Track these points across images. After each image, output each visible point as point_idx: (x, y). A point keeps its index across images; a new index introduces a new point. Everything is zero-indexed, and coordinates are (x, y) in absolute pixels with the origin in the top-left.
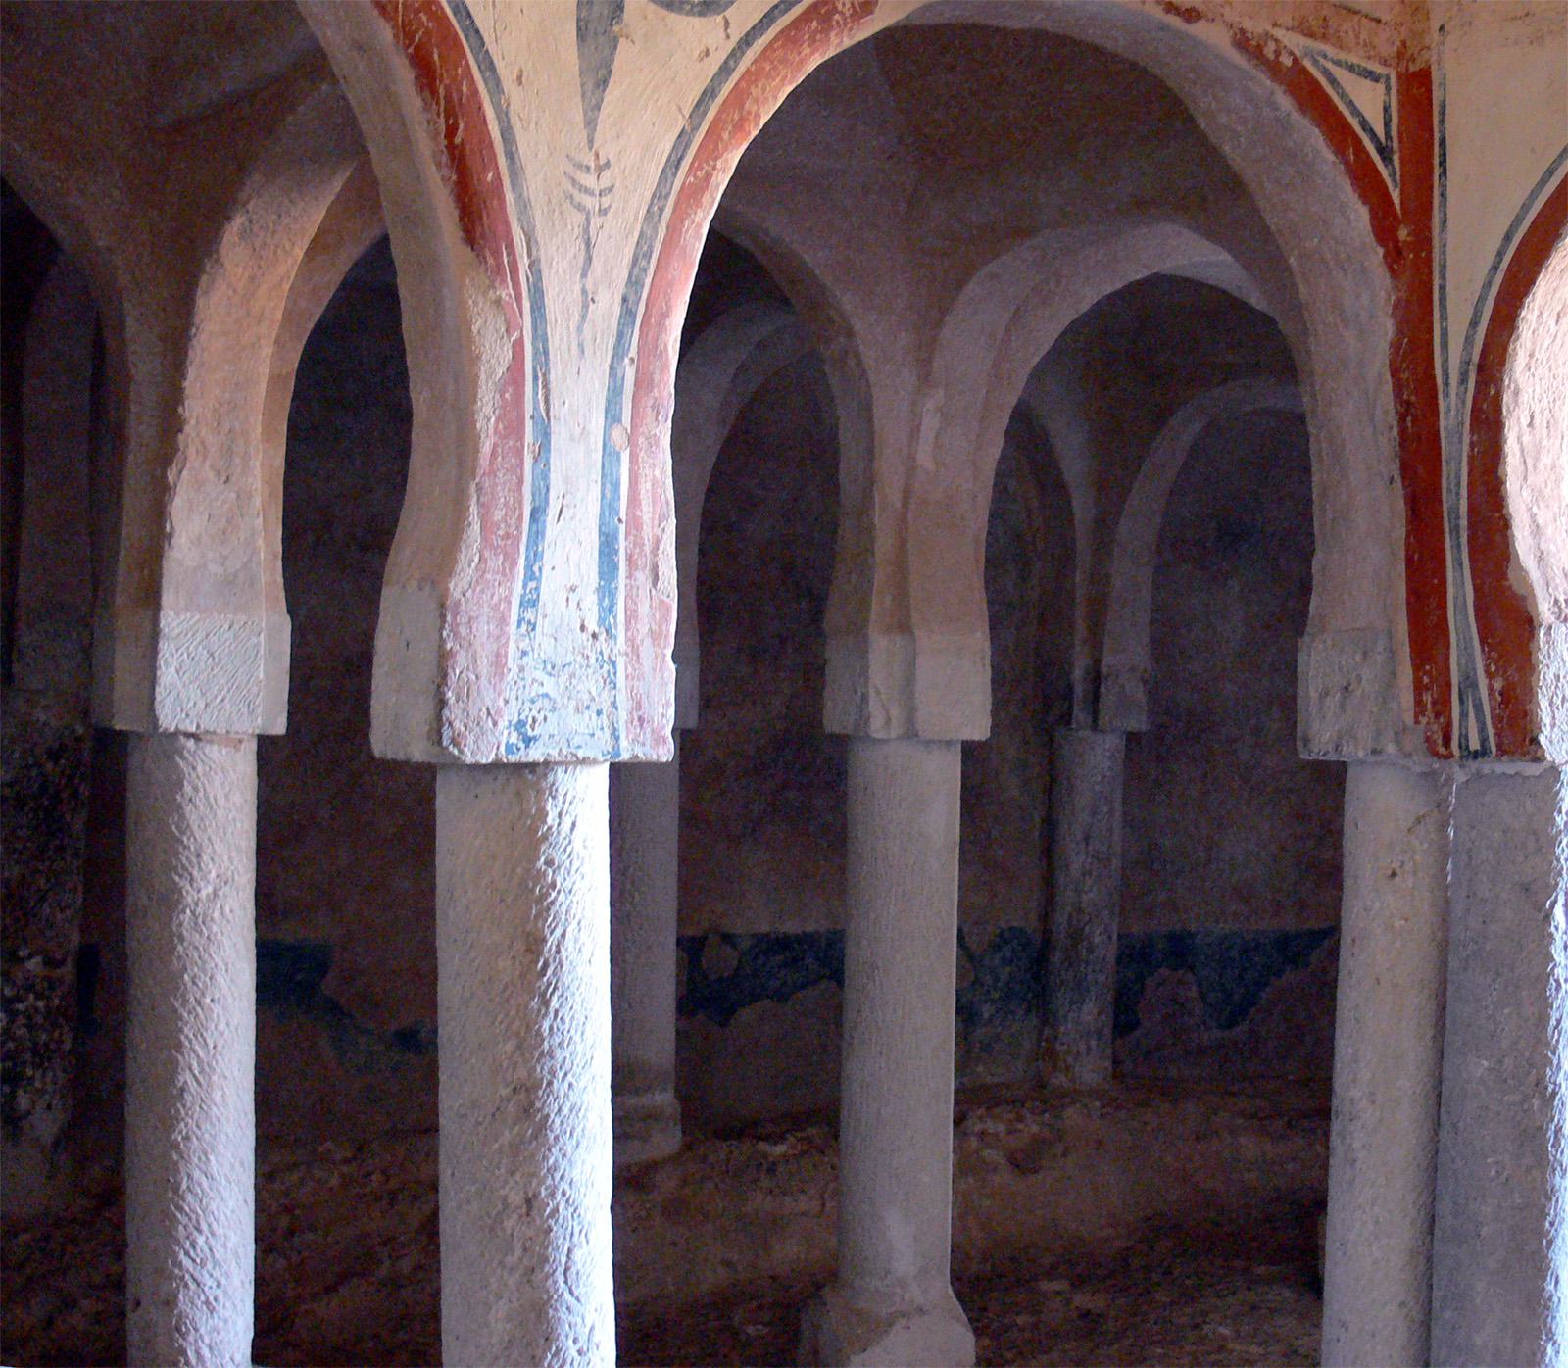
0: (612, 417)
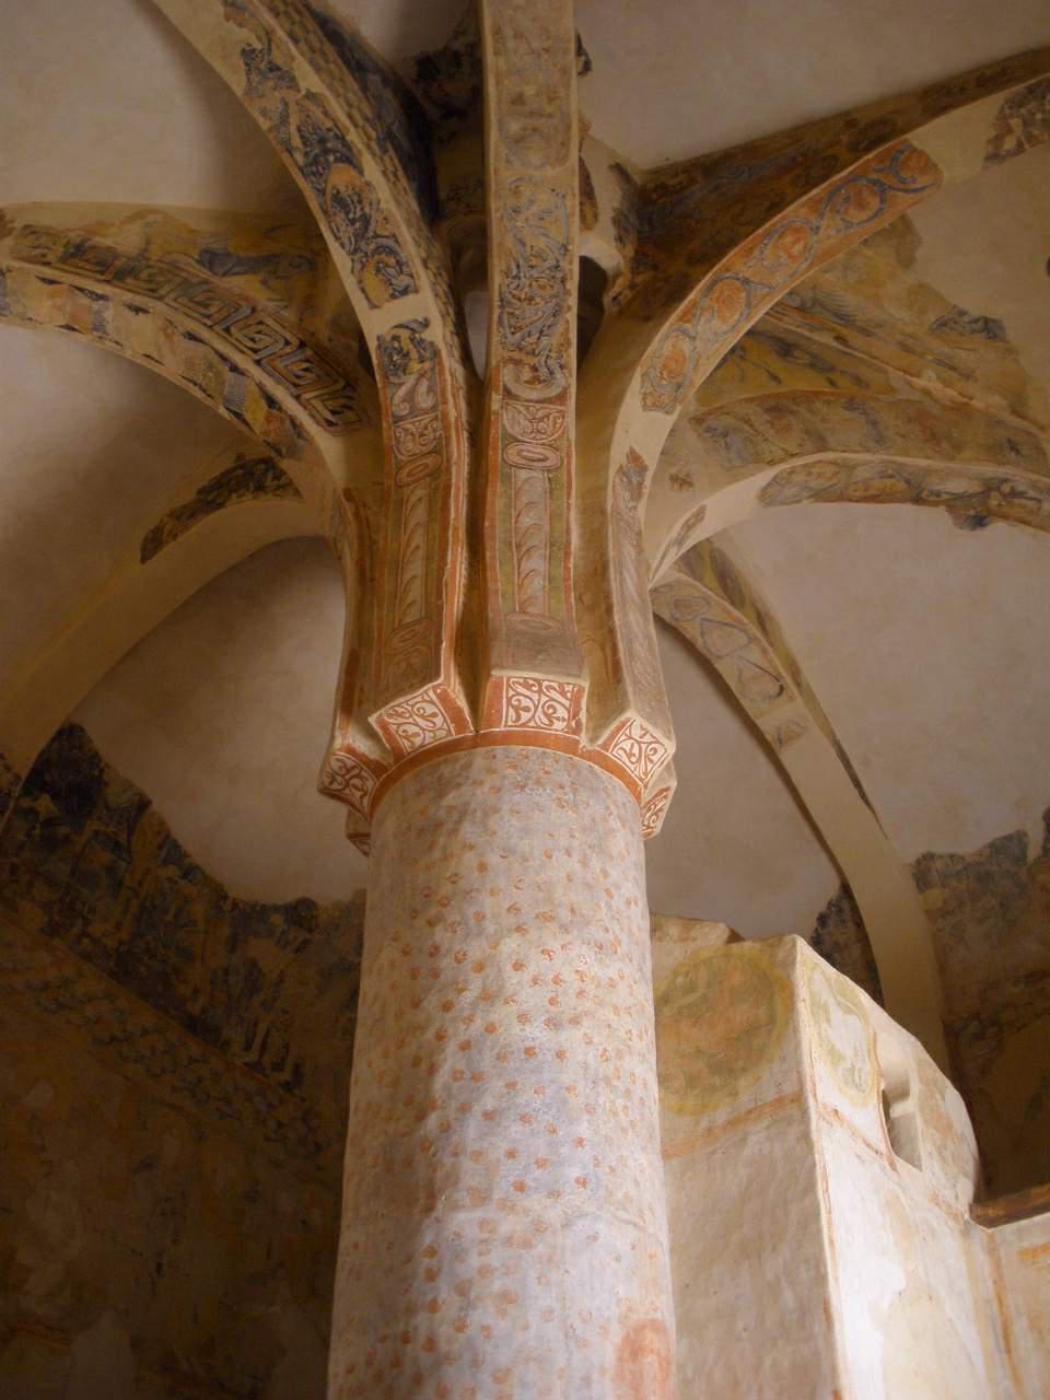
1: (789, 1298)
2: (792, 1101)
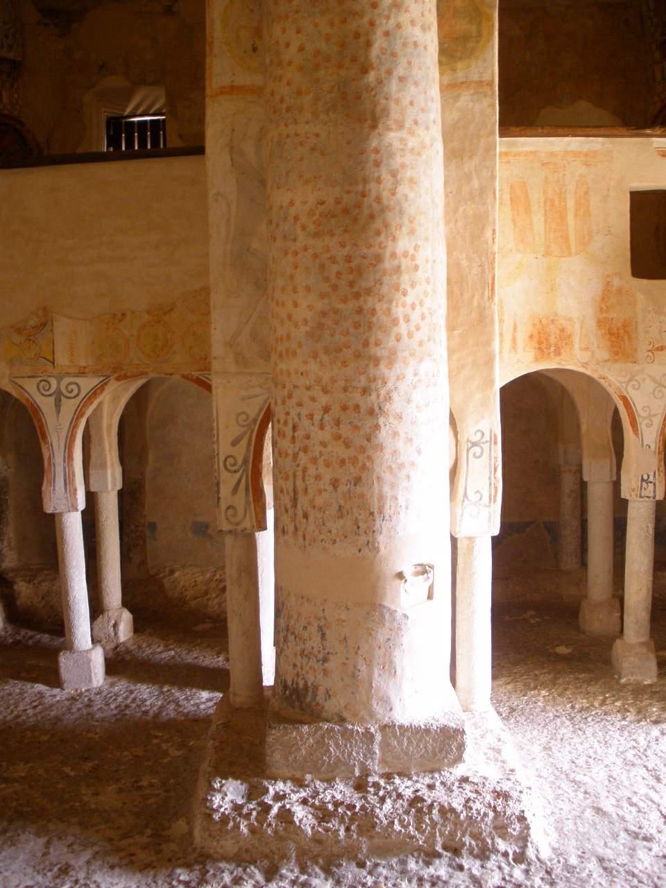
0: (64, 461)
1: (476, 183)
2: (487, 84)
